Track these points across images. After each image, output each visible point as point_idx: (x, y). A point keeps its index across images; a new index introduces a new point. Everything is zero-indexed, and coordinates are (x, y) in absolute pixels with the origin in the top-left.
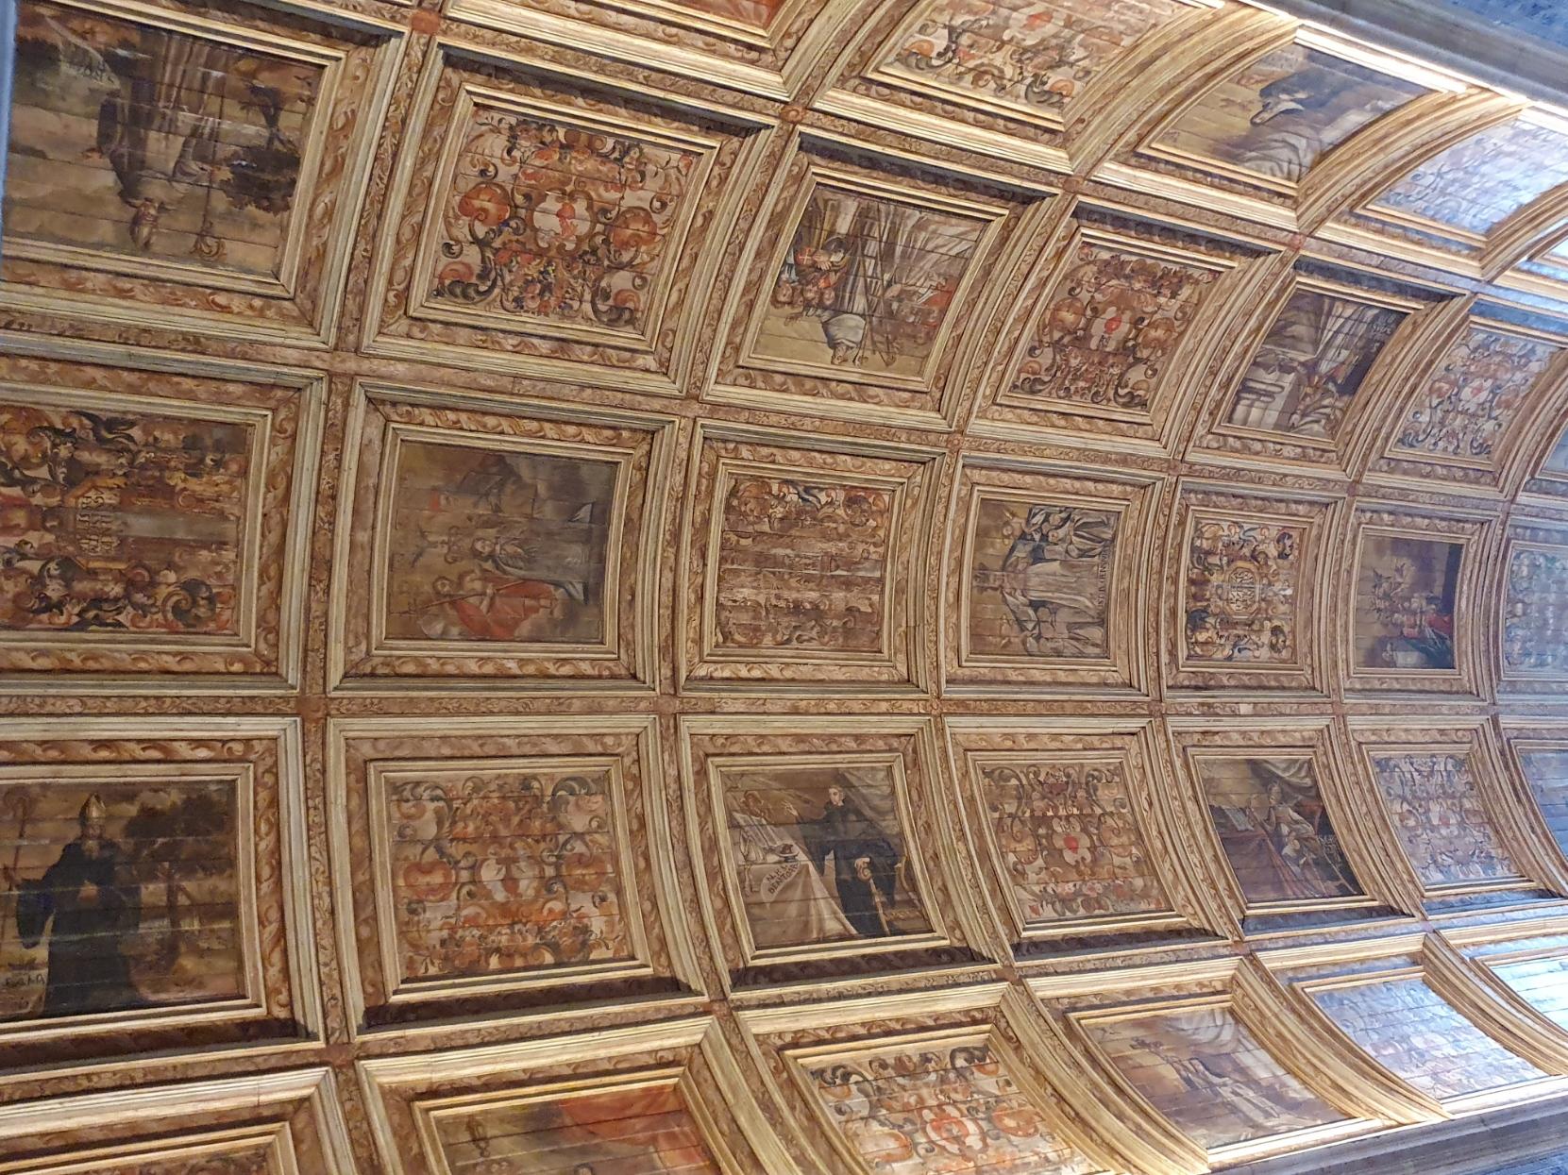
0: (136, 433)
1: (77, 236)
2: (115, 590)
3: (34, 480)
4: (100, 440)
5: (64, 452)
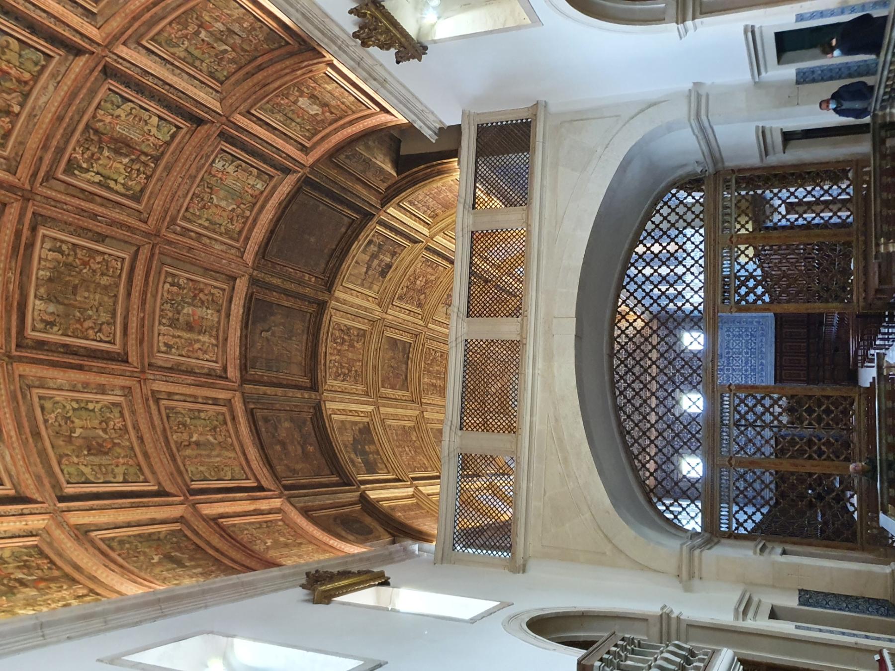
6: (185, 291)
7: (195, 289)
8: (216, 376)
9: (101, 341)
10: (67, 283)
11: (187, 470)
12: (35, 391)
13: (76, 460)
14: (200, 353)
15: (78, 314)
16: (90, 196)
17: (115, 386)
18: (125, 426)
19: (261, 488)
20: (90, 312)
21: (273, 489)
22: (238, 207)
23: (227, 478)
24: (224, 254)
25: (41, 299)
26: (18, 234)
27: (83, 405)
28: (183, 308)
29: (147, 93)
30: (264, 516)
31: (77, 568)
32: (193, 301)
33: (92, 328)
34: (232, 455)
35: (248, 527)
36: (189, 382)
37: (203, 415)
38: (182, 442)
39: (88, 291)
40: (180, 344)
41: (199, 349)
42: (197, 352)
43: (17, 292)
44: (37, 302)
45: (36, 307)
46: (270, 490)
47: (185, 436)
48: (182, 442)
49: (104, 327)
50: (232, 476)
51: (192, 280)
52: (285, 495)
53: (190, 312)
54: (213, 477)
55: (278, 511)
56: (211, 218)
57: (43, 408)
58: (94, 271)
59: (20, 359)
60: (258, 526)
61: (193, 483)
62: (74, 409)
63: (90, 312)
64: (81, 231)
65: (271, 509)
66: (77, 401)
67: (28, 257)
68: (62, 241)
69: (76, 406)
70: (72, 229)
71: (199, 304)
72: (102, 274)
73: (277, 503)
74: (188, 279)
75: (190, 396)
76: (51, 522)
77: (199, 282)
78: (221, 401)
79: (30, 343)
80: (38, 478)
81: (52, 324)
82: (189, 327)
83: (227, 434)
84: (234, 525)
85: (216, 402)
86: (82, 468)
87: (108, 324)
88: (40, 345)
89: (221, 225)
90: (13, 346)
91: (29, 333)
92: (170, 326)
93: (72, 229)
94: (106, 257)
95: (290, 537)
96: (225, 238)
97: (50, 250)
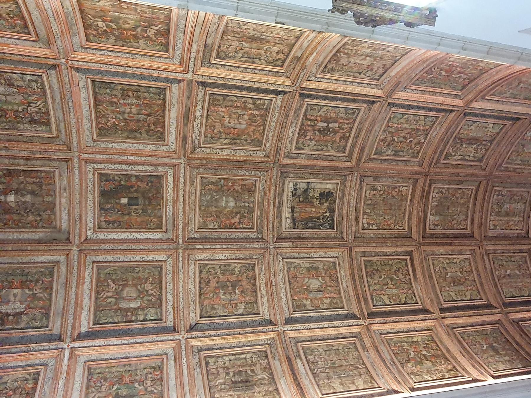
9: (461, 229)
10: (445, 205)
12: (430, 257)
13: (448, 289)
15: (450, 219)
16: (456, 166)
17: (466, 250)
18: (471, 269)
20: (455, 217)
25: (433, 215)
26: (423, 191)
27: (451, 261)
28: (504, 206)
29: (487, 116)
31: (448, 351)
33: (456, 223)
36: (505, 243)
39: (454, 207)
43: (423, 214)
44: (431, 217)
45: (431, 218)
49: (462, 222)
57: (433, 264)
58: (457, 198)
59: (424, 244)
62: (447, 263)
63: (455, 217)
64: (450, 182)
66: (449, 259)
67: (427, 198)
68: (442, 188)
69: (448, 262)
70: (447, 182)
72: (461, 198)
75: (506, 250)
76: (437, 323)
79: (428, 235)
80: (432, 301)
81: (437, 225)
82: (507, 214)
86: (451, 293)
87: (464, 220)
88: (432, 235)
90: (421, 238)
91: (428, 230)
93: (447, 182)
94: (464, 190)
97: (437, 193)
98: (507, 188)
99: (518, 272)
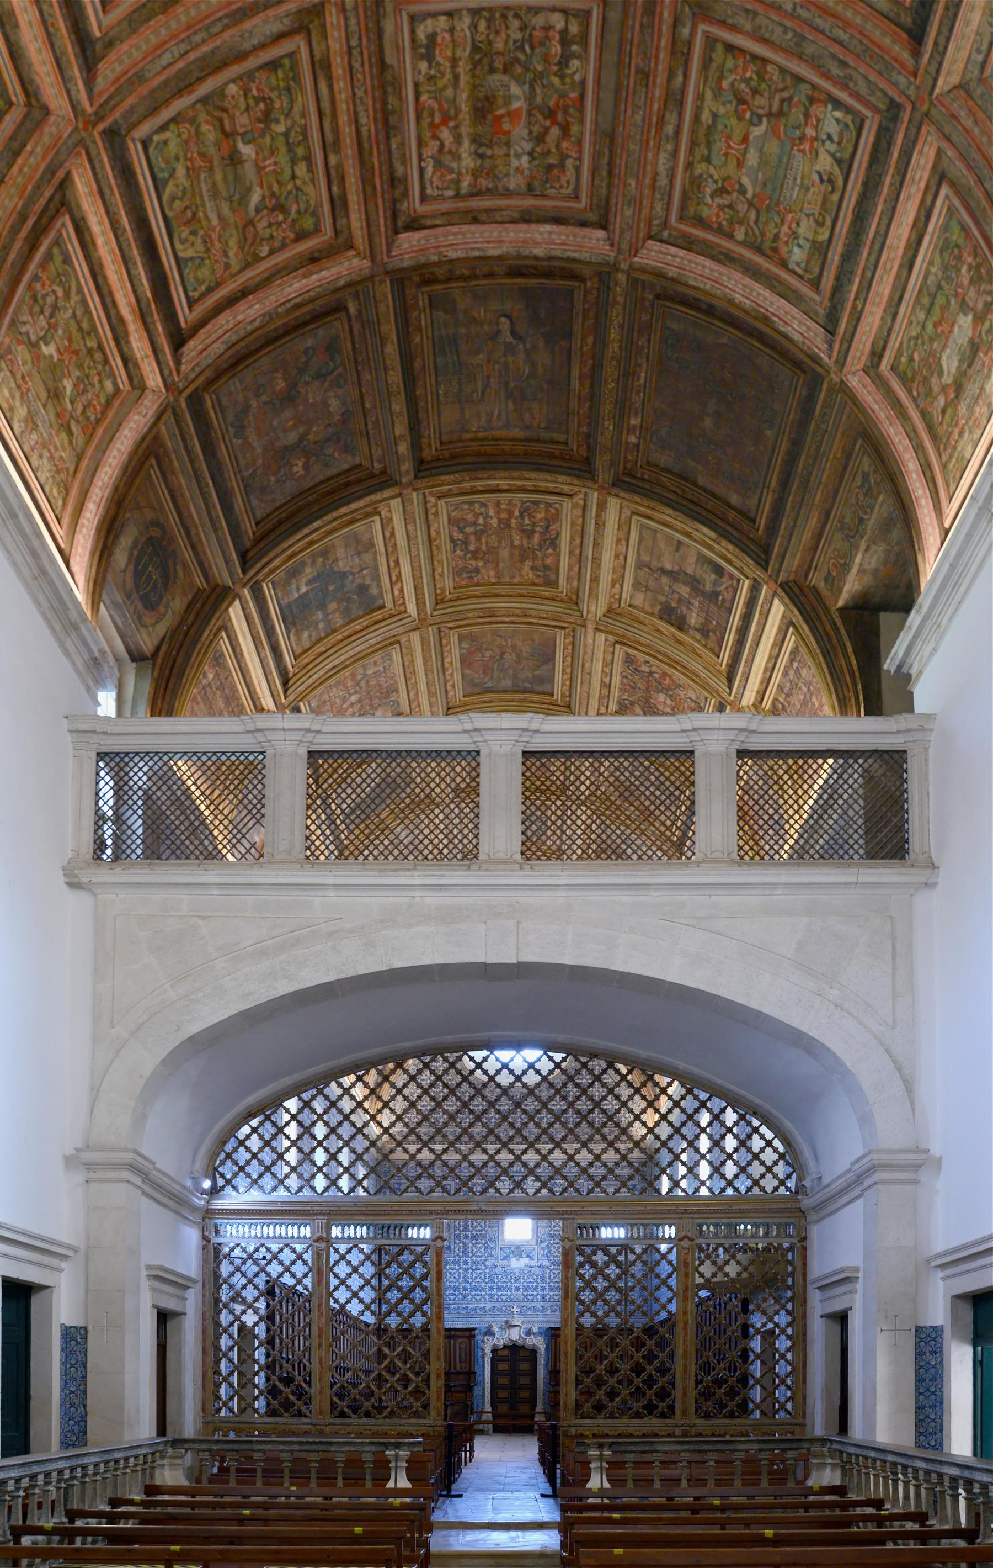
0: (550, 551)
1: (642, 548)
2: (472, 548)
3: (523, 518)
4: (545, 540)
5: (538, 529)
6: (556, 80)
7: (566, 112)
8: (394, 201)
11: (164, 128)
14: (431, 148)
19: (179, 341)
21: (183, 367)
22: (751, 204)
23: (178, 246)
24: (647, 181)
28: (520, 81)
30: (112, 343)
32: (540, 109)
34: (235, 264)
35: (75, 298)
36: (363, 120)
37: (301, 170)
38: (224, 110)
40: (441, 83)
41: (442, 145)
42: (435, 137)
46: (178, 363)
47: (243, 121)
48: (224, 110)
50: (187, 260)
51: (582, 97)
52: (177, 401)
53: (516, 105)
54: (171, 209)
55: (139, 386)
56: (720, 127)
60: (85, 325)
61: (139, 146)
65: (137, 365)
71: (536, 129)
73: (153, 379)
74: (583, 83)
75: (336, 130)
77: (582, 121)
78: (345, 221)
83: (277, 244)
84: (67, 260)
85: (339, 205)
89: (708, 160)
92: (475, 49)
95: (80, 408)
96: (683, 179)
98: (598, 82)
99: (255, 198)
